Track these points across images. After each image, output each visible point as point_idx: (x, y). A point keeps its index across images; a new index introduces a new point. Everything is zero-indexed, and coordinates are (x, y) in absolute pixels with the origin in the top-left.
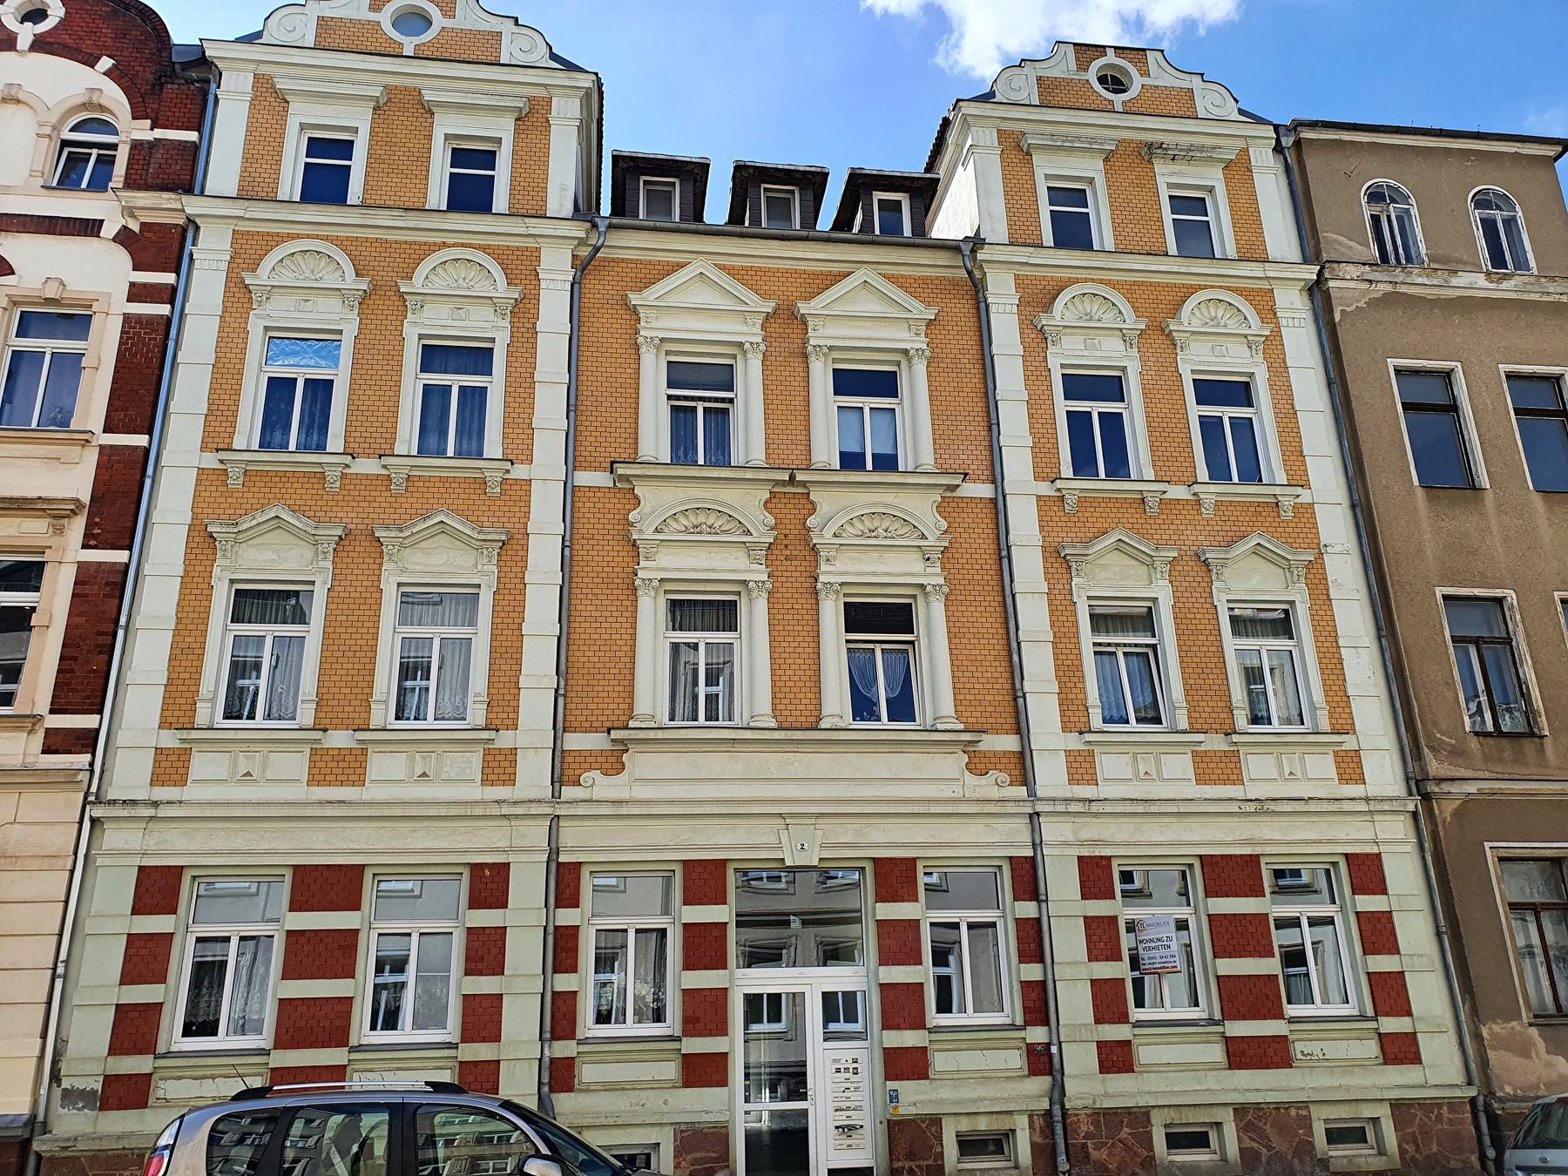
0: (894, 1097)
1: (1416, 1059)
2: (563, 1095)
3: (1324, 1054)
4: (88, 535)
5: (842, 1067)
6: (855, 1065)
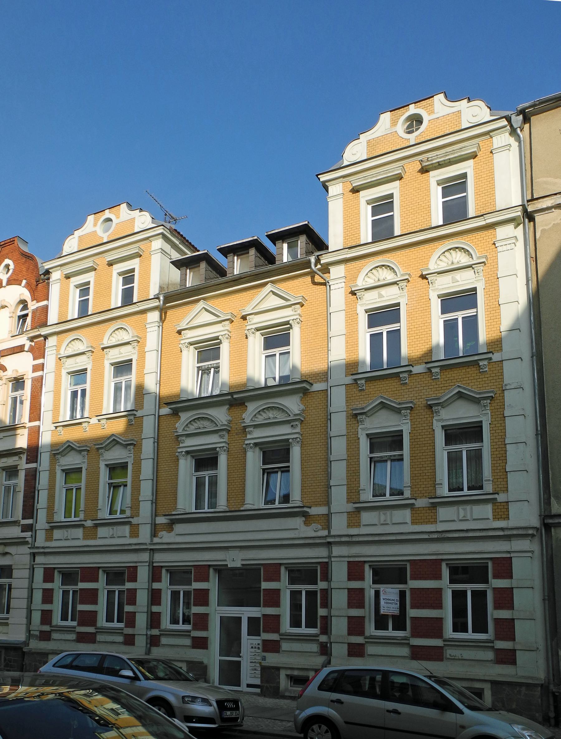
0: (264, 658)
1: (513, 662)
2: (155, 648)
3: (462, 657)
4: (27, 459)
5: (254, 646)
6: (259, 646)
